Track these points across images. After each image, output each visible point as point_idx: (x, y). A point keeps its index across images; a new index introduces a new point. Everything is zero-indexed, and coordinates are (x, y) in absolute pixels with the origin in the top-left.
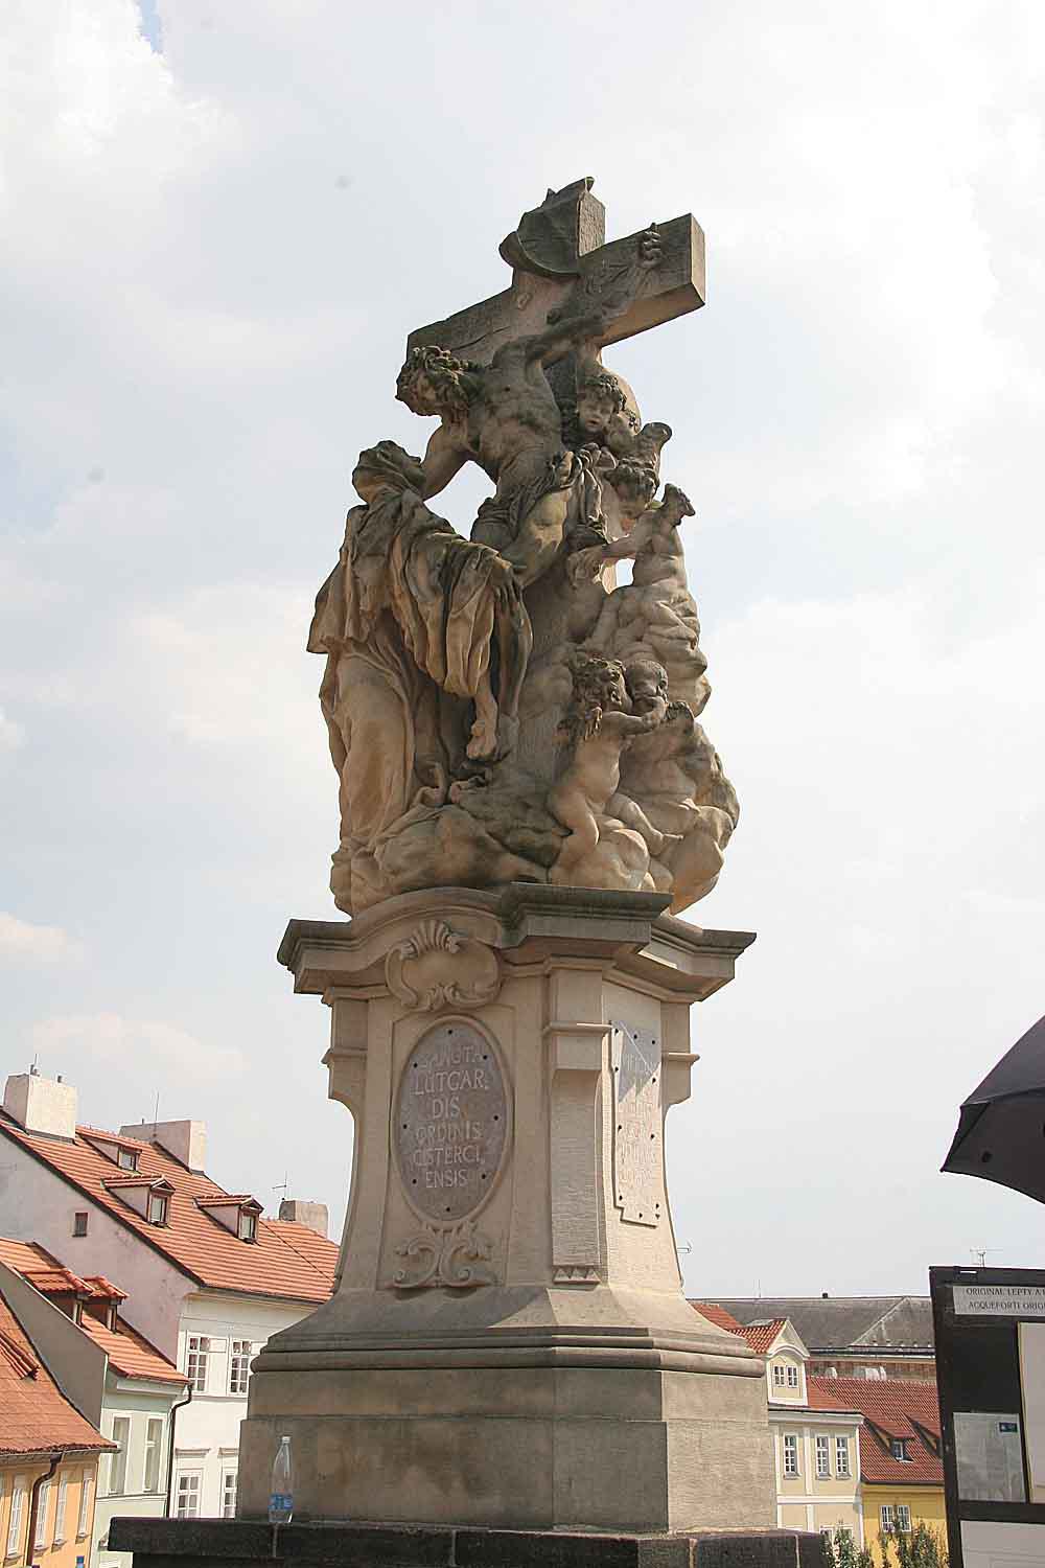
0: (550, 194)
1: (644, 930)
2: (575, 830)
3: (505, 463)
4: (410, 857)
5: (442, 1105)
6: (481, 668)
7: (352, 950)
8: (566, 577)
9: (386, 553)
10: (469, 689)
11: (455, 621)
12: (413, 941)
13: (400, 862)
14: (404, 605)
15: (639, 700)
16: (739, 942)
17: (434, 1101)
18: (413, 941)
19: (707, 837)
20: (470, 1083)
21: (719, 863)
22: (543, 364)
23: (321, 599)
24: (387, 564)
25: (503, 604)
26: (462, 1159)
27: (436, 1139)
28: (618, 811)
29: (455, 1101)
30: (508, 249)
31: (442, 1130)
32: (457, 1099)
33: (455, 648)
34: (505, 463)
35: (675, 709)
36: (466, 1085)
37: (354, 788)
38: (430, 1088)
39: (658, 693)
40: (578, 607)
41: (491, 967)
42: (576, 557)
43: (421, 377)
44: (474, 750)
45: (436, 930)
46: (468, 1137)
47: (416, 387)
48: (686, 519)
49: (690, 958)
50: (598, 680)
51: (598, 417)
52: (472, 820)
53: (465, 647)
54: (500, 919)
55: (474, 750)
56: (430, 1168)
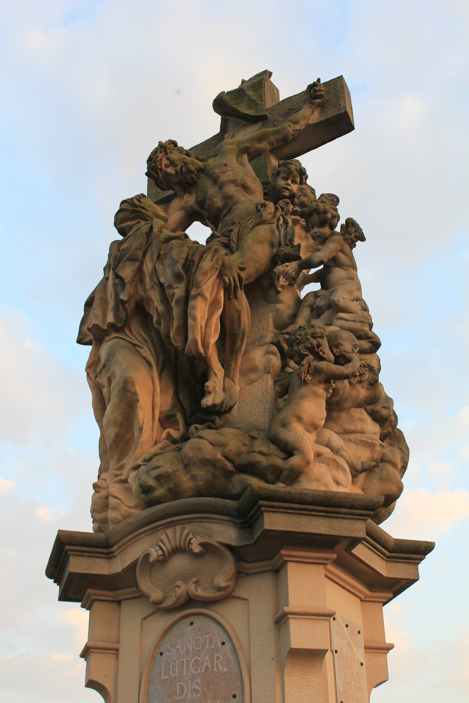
0: (243, 82)
1: (358, 528)
2: (296, 452)
3: (224, 212)
4: (158, 478)
5: (185, 688)
6: (213, 339)
7: (109, 556)
8: (273, 286)
9: (140, 259)
10: (205, 353)
11: (195, 297)
12: (160, 544)
13: (151, 482)
14: (155, 295)
15: (339, 356)
16: (419, 550)
17: (178, 684)
18: (160, 544)
19: (390, 468)
20: (209, 665)
21: (400, 489)
22: (248, 157)
23: (89, 304)
24: (142, 264)
25: (230, 292)
28: (327, 440)
29: (197, 683)
30: (220, 104)
32: (199, 681)
33: (194, 319)
34: (224, 212)
35: (365, 366)
36: (207, 667)
37: (112, 432)
38: (174, 672)
39: (353, 352)
40: (280, 306)
41: (229, 567)
42: (280, 268)
43: (164, 159)
44: (207, 401)
45: (181, 535)
47: (160, 165)
48: (359, 243)
49: (384, 562)
50: (309, 337)
51: (290, 185)
52: (211, 446)
54: (238, 521)
55: (207, 401)
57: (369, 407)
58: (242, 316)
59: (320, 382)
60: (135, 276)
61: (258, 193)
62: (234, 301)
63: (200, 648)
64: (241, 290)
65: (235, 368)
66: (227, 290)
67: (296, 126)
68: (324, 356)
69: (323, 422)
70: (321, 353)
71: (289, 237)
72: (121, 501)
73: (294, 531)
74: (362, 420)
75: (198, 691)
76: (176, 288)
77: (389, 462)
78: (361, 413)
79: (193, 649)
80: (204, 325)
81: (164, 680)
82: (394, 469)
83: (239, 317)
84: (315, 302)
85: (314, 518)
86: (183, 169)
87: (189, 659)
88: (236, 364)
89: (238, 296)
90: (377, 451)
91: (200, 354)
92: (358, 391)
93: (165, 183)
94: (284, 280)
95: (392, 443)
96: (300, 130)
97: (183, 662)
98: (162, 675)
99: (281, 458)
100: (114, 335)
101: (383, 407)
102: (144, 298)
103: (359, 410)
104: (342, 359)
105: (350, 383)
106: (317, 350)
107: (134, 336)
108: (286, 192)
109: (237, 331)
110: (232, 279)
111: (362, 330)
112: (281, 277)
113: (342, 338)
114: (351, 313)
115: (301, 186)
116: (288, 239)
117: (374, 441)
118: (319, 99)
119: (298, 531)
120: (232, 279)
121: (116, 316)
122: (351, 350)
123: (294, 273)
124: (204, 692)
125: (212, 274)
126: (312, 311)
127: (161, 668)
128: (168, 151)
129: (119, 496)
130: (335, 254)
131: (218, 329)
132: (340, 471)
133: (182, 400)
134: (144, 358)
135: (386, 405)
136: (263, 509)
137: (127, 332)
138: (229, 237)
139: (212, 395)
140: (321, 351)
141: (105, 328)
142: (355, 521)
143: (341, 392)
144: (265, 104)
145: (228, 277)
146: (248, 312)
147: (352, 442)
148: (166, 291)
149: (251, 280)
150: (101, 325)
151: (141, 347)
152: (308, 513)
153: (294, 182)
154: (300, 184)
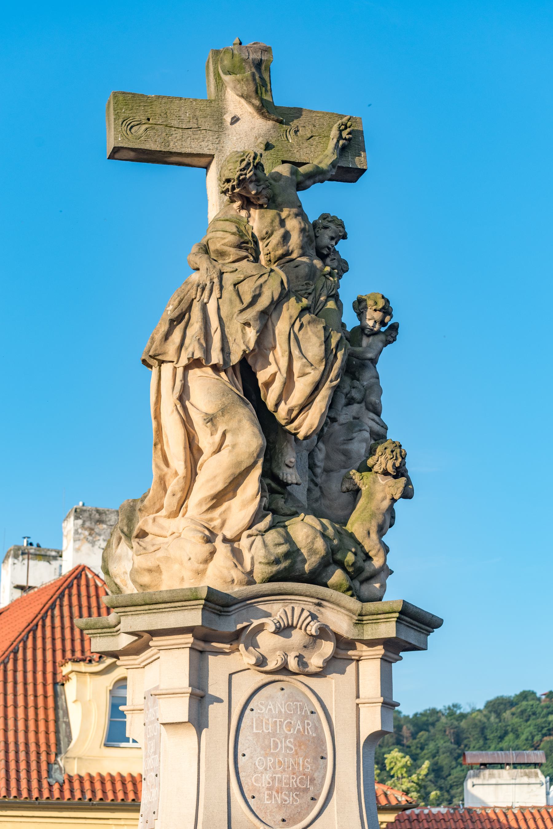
20: (301, 730)
26: (297, 785)
27: (275, 768)
31: (280, 762)
36: (299, 730)
46: (301, 769)
56: (269, 789)
63: (292, 712)
75: (291, 749)
79: (285, 712)
81: (256, 734)
84: (350, 392)
87: (282, 720)
97: (276, 722)
98: (254, 729)
124: (296, 750)
127: (253, 723)
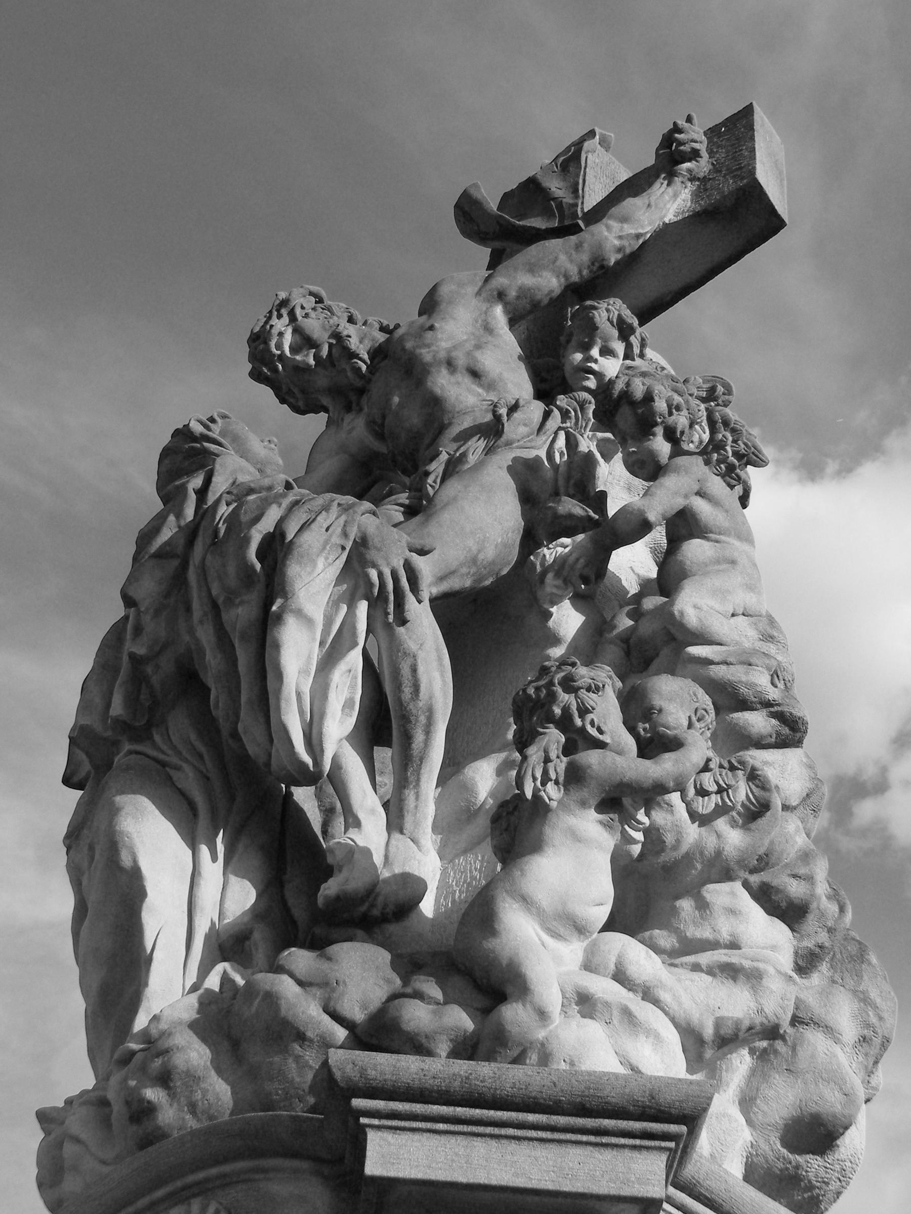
3: (427, 441)
14: (205, 635)
22: (506, 311)
24: (184, 565)
47: (279, 346)
51: (596, 361)
53: (304, 672)
57: (754, 879)
58: (421, 669)
59: (583, 804)
60: (167, 595)
61: (510, 385)
62: (401, 630)
64: (420, 602)
65: (416, 807)
66: (377, 602)
67: (626, 226)
68: (601, 737)
69: (603, 913)
70: (593, 732)
71: (577, 475)
72: (86, 1146)
73: (449, 1179)
74: (732, 912)
76: (242, 603)
77: (815, 1023)
78: (733, 894)
80: (306, 689)
82: (830, 1042)
83: (414, 670)
85: (513, 1146)
86: (334, 351)
88: (417, 797)
89: (409, 615)
90: (772, 992)
91: (303, 765)
92: (719, 836)
93: (296, 391)
94: (559, 582)
95: (837, 977)
96: (638, 236)
99: (478, 1009)
100: (127, 747)
101: (795, 876)
102: (193, 647)
103: (725, 887)
104: (654, 744)
105: (693, 815)
106: (578, 722)
107: (174, 748)
108: (588, 379)
109: (411, 706)
110: (387, 573)
111: (751, 685)
112: (550, 576)
113: (660, 694)
114: (721, 645)
115: (628, 362)
116: (572, 482)
117: (761, 966)
118: (690, 160)
119: (462, 1179)
120: (387, 573)
121: (132, 701)
122: (685, 723)
123: (582, 561)
125: (330, 560)
126: (628, 653)
128: (299, 312)
129: (83, 1136)
130: (679, 503)
131: (354, 703)
132: (642, 1038)
133: (291, 902)
134: (182, 793)
135: (802, 871)
136: (363, 1120)
137: (157, 738)
138: (420, 490)
139: (344, 874)
140: (592, 723)
141: (109, 733)
142: (636, 1154)
143: (669, 839)
144: (582, 203)
145: (374, 566)
146: (440, 659)
147: (702, 970)
148: (225, 617)
149: (454, 584)
150: (98, 727)
151: (178, 768)
152: (496, 1131)
153: (606, 351)
154: (626, 357)
